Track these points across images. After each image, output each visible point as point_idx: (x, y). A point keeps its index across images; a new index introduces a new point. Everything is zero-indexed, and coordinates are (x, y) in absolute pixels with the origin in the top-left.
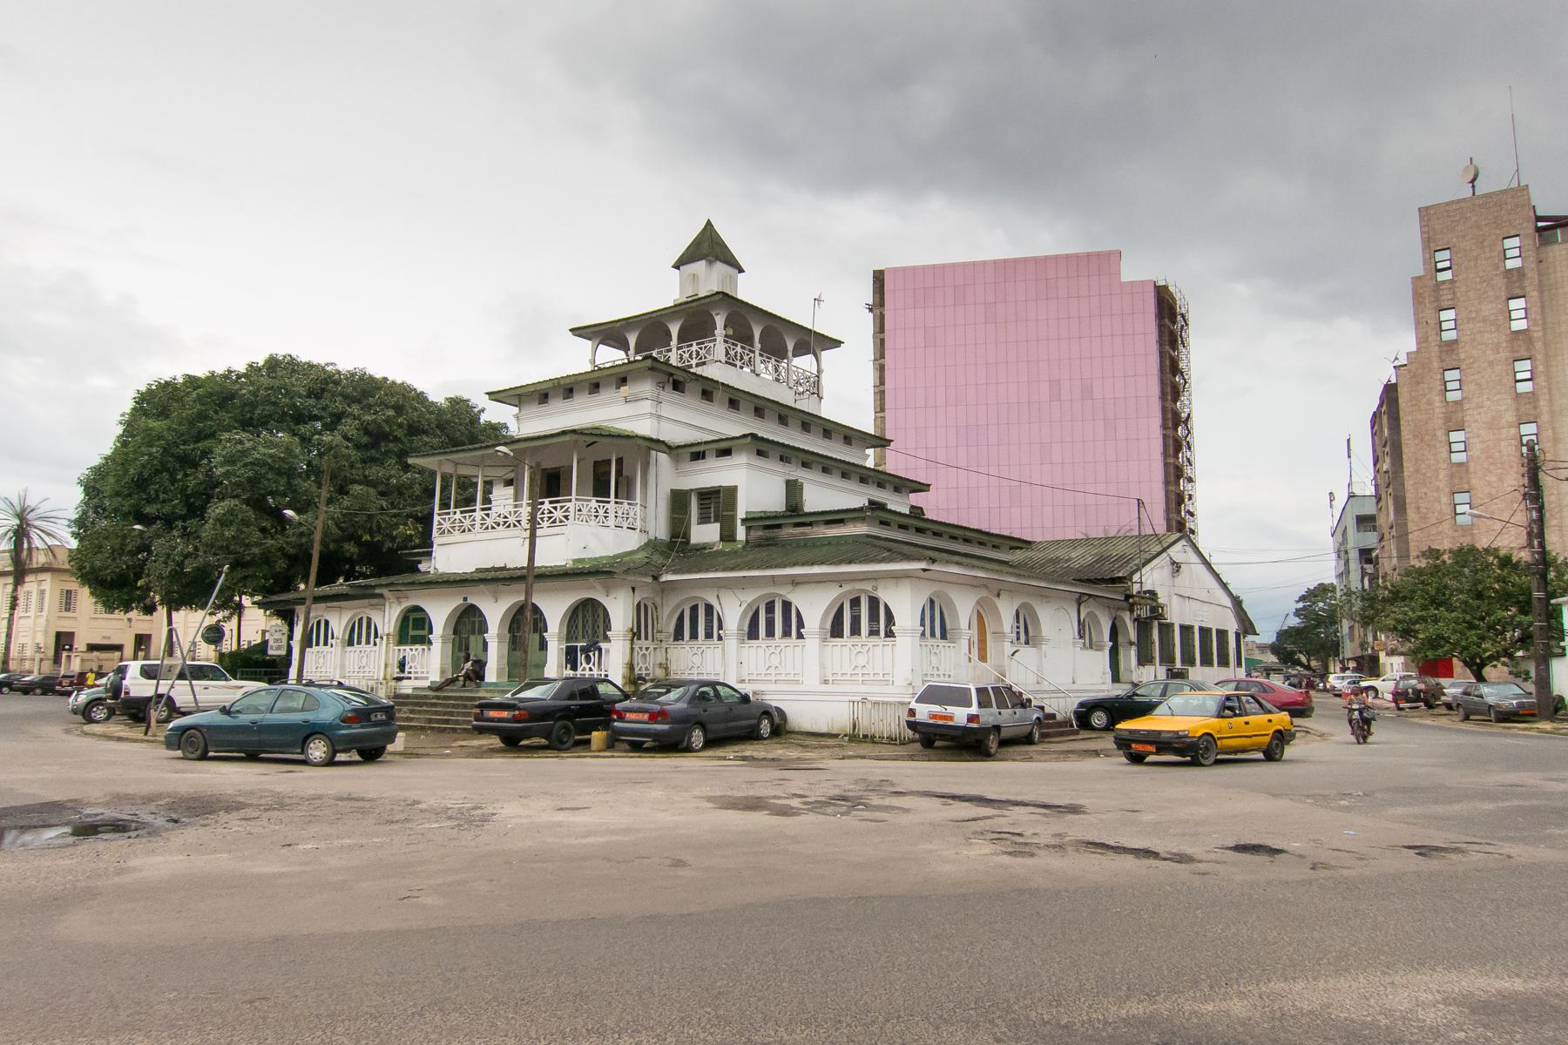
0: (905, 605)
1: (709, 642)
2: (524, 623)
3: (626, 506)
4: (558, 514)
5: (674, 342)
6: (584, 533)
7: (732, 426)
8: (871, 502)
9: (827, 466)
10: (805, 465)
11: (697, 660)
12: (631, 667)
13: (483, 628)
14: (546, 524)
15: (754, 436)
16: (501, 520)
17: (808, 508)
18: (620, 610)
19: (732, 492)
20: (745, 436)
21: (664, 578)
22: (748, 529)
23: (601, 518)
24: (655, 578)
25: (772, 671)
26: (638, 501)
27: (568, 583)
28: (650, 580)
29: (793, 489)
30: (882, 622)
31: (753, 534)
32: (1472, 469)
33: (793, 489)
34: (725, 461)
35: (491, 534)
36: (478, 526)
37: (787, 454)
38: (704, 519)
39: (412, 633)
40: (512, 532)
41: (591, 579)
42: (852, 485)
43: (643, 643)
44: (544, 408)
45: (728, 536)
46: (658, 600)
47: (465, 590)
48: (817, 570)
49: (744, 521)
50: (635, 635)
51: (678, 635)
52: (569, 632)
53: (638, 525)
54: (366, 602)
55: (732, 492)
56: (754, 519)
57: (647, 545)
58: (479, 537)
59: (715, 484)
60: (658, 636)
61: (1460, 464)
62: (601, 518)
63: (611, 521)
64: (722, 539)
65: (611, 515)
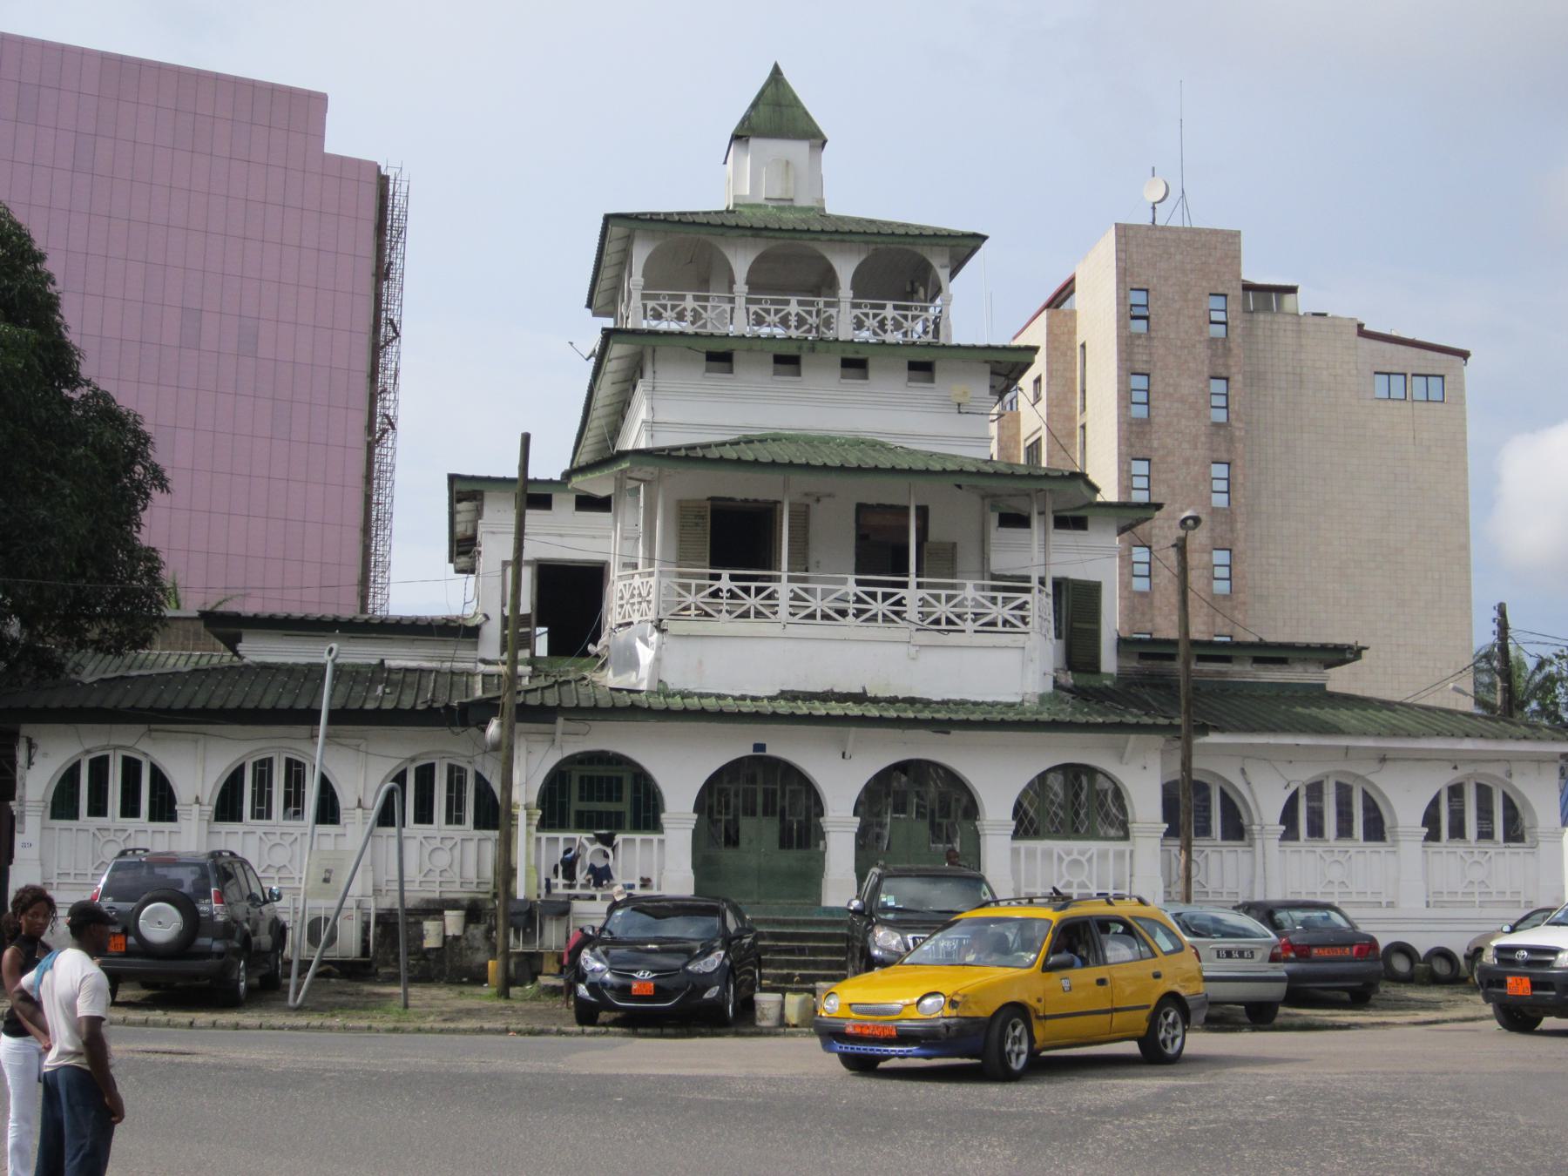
5: (845, 292)
13: (815, 804)
16: (852, 608)
35: (818, 629)
39: (576, 805)
40: (878, 630)
47: (760, 733)
48: (1468, 745)
61: (1142, 594)
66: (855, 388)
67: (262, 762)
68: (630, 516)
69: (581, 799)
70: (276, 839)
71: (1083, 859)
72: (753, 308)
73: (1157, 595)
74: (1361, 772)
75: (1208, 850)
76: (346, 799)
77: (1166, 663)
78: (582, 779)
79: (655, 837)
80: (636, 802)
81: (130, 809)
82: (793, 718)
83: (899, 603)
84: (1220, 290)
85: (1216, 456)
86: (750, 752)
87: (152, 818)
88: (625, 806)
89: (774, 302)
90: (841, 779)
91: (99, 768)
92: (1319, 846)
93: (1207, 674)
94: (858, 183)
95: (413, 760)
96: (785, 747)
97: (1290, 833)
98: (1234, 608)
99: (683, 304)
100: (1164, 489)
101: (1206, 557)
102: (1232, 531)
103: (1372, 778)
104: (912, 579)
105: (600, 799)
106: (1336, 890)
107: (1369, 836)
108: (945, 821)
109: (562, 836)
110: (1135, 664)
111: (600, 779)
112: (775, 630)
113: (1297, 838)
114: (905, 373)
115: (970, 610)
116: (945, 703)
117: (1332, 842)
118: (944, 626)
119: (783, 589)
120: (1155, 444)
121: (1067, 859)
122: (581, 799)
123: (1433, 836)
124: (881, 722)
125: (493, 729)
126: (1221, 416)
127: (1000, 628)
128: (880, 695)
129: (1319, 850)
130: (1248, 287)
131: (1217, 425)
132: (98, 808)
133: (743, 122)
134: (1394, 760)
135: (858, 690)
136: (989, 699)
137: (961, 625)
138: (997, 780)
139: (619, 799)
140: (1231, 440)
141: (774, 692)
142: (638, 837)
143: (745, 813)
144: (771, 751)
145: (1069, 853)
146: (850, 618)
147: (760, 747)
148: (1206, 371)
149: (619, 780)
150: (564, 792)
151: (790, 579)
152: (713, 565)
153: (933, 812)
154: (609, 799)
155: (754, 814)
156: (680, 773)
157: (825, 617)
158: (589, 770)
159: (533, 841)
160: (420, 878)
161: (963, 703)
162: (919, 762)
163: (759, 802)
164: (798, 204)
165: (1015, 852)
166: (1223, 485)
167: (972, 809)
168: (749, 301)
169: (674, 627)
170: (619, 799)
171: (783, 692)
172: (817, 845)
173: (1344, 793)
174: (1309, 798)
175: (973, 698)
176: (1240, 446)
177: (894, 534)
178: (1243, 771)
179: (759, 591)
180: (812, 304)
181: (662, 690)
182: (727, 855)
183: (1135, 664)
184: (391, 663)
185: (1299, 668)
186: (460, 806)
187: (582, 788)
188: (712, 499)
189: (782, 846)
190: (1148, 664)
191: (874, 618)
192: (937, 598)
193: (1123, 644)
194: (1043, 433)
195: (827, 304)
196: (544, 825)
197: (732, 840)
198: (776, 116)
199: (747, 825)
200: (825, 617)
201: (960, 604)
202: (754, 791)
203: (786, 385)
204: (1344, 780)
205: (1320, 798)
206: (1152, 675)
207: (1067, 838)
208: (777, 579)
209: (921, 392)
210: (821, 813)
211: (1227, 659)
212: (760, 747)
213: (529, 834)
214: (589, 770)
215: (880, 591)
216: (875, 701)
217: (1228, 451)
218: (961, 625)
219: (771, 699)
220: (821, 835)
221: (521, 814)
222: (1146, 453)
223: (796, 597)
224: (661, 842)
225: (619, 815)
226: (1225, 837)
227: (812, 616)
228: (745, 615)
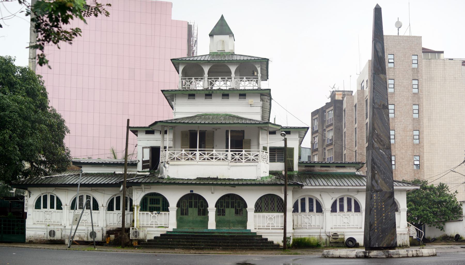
1: (311, 213)
5: (233, 75)
11: (306, 220)
14: (243, 161)
21: (304, 187)
25: (346, 224)
32: (396, 147)
35: (206, 162)
39: (149, 205)
44: (192, 101)
47: (192, 188)
54: (90, 188)
58: (200, 163)
66: (226, 101)
67: (81, 196)
68: (169, 137)
69: (150, 204)
71: (273, 217)
72: (209, 80)
73: (396, 144)
74: (352, 195)
75: (312, 215)
76: (100, 204)
77: (312, 168)
78: (150, 199)
79: (167, 213)
80: (163, 205)
81: (52, 207)
82: (200, 184)
83: (226, 155)
84: (416, 54)
85: (414, 103)
86: (189, 192)
87: (57, 209)
88: (160, 206)
89: (215, 79)
90: (212, 199)
91: (45, 197)
92: (342, 214)
94: (243, 46)
95: (115, 195)
96: (197, 191)
98: (420, 148)
99: (192, 80)
100: (399, 113)
101: (411, 133)
102: (419, 125)
103: (355, 196)
105: (155, 204)
106: (346, 224)
107: (355, 211)
108: (239, 209)
109: (145, 212)
110: (304, 168)
111: (155, 199)
112: (195, 163)
113: (336, 211)
114: (238, 98)
115: (243, 157)
116: (238, 180)
117: (346, 213)
118: (237, 161)
119: (198, 153)
120: (396, 100)
121: (268, 217)
122: (150, 204)
124: (221, 185)
125: (122, 188)
126: (416, 91)
127: (251, 161)
128: (221, 178)
129: (341, 215)
130: (425, 51)
131: (414, 94)
132: (45, 207)
133: (212, 31)
134: (361, 191)
135: (216, 177)
136: (249, 178)
137: (242, 161)
138: (251, 199)
139: (159, 204)
140: (419, 98)
141: (195, 178)
142: (163, 213)
143: (190, 207)
144: (194, 192)
145: (269, 216)
146: (214, 160)
147: (192, 191)
148: (411, 78)
149: (159, 200)
150: (146, 202)
151: (199, 151)
152: (182, 148)
153: (236, 206)
154: (157, 204)
155: (192, 207)
156: (173, 198)
157: (208, 159)
158: (152, 197)
159: (138, 214)
160: (117, 223)
161: (242, 180)
162: (230, 194)
163: (193, 204)
164: (226, 51)
165: (255, 216)
166: (417, 112)
167: (245, 206)
168: (208, 79)
169: (171, 163)
170: (159, 204)
171: (197, 178)
172: (207, 215)
173: (349, 201)
174: (340, 202)
175: (244, 178)
176: (421, 100)
177: (238, 138)
178: (320, 195)
179: (192, 153)
180: (225, 78)
181: (169, 179)
182: (185, 217)
183: (304, 168)
184: (117, 173)
185: (348, 168)
186: (126, 206)
187: (150, 202)
188: (190, 131)
189: (199, 215)
190: (307, 168)
191: (220, 159)
192: (236, 154)
193: (300, 164)
194: (368, 97)
195: (228, 78)
196: (141, 210)
197: (187, 214)
198: (222, 28)
199: (190, 210)
200: (208, 159)
201: (241, 155)
202: (192, 202)
203: (208, 101)
204: (349, 197)
205: (343, 202)
206: (308, 171)
207: (269, 212)
208: (196, 151)
209: (243, 101)
210: (208, 206)
211: (329, 167)
213: (137, 212)
214: (152, 197)
215: (237, 153)
216: (220, 179)
217: (418, 101)
218: (242, 161)
219: (195, 180)
220: (208, 212)
221: (136, 207)
222: (393, 103)
223: (201, 155)
224: (169, 214)
225: (159, 208)
226: (317, 212)
227: (204, 159)
228: (188, 159)
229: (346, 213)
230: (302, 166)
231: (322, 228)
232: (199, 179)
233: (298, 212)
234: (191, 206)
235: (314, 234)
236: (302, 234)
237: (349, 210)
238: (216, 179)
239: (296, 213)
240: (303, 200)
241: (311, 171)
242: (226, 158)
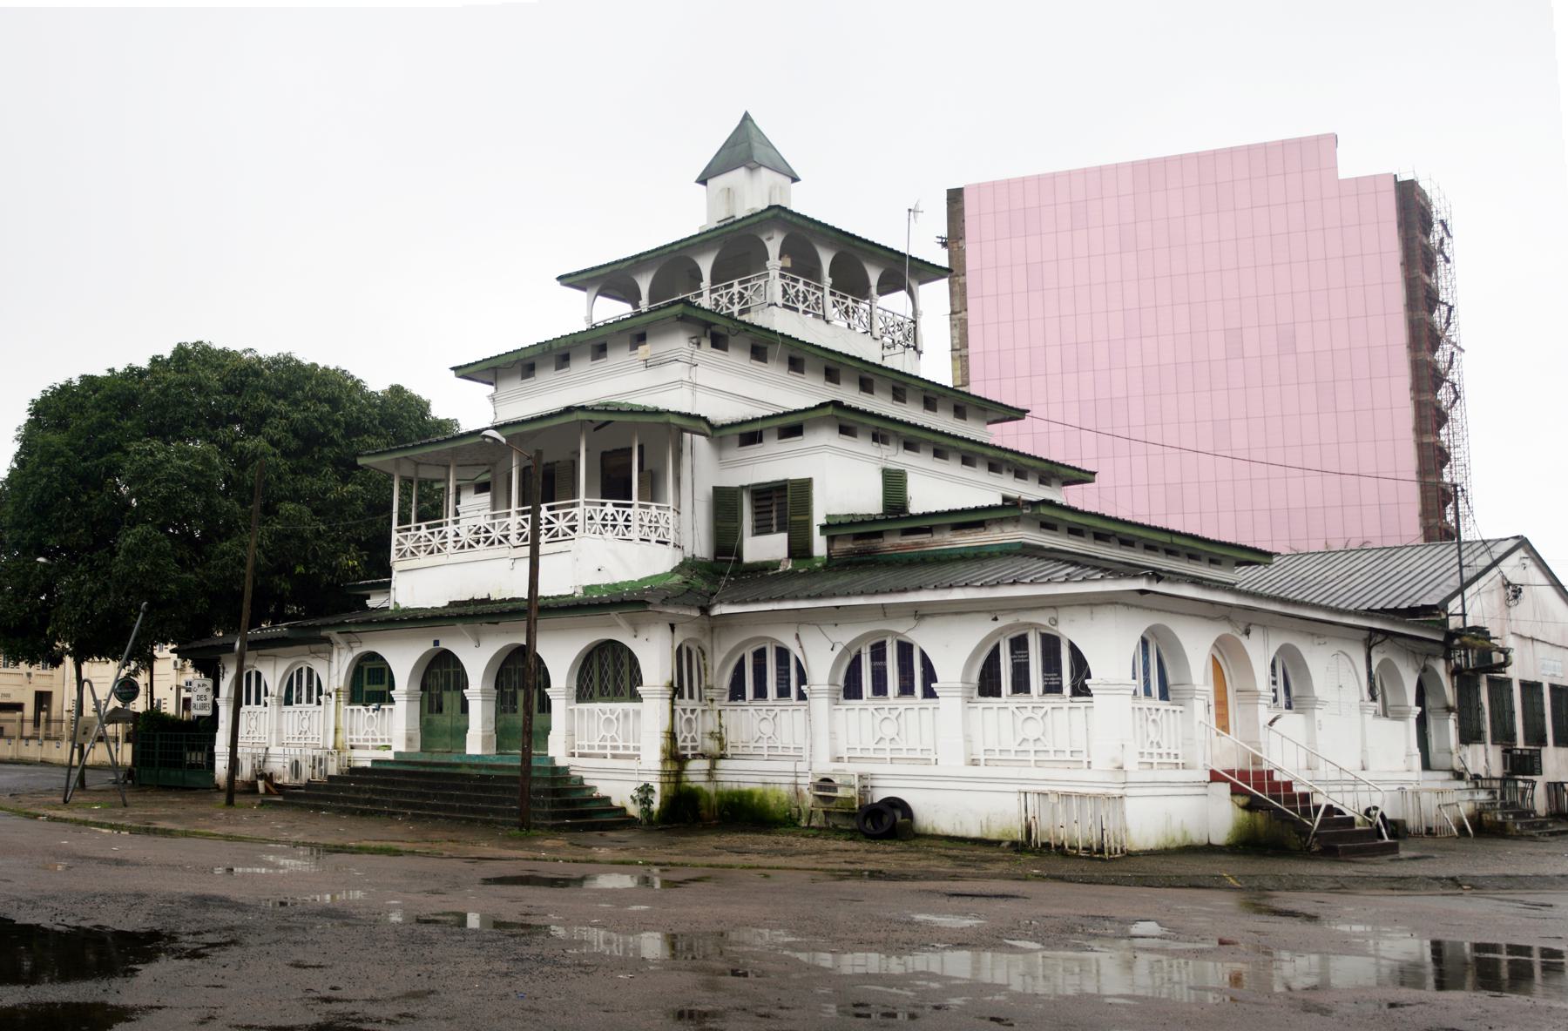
0: (1109, 645)
2: (520, 678)
3: (654, 511)
4: (561, 525)
6: (600, 551)
7: (802, 393)
8: (1005, 499)
9: (942, 447)
10: (910, 446)
12: (672, 736)
15: (837, 404)
17: (915, 507)
18: (654, 655)
19: (804, 487)
20: (822, 406)
22: (831, 540)
23: (621, 528)
24: (705, 610)
26: (671, 504)
27: (577, 619)
28: (696, 613)
29: (894, 482)
30: (1072, 675)
31: (839, 546)
33: (894, 482)
34: (793, 444)
35: (467, 555)
36: (450, 544)
37: (882, 431)
38: (762, 528)
40: (497, 551)
41: (613, 613)
42: (980, 474)
43: (685, 703)
45: (800, 549)
46: (706, 643)
49: (823, 528)
50: (676, 691)
51: (737, 692)
52: (580, 687)
53: (671, 537)
55: (804, 487)
56: (840, 525)
57: (682, 565)
58: (453, 559)
59: (781, 478)
60: (709, 693)
62: (621, 528)
63: (635, 533)
64: (791, 555)
65: (635, 524)
70: (1028, 713)
93: (906, 547)
97: (852, 689)
104: (515, 507)
123: (852, 689)
144: (442, 645)
147: (436, 643)
183: (850, 546)
190: (860, 544)
206: (861, 553)
207: (612, 701)
212: (436, 643)
229: (892, 700)
230: (844, 538)
231: (799, 758)
232: (453, 604)
233: (743, 698)
234: (448, 689)
235: (777, 779)
236: (741, 778)
237: (1052, 688)
238: (487, 601)
239: (740, 702)
240: (760, 656)
241: (869, 553)
242: (506, 537)
